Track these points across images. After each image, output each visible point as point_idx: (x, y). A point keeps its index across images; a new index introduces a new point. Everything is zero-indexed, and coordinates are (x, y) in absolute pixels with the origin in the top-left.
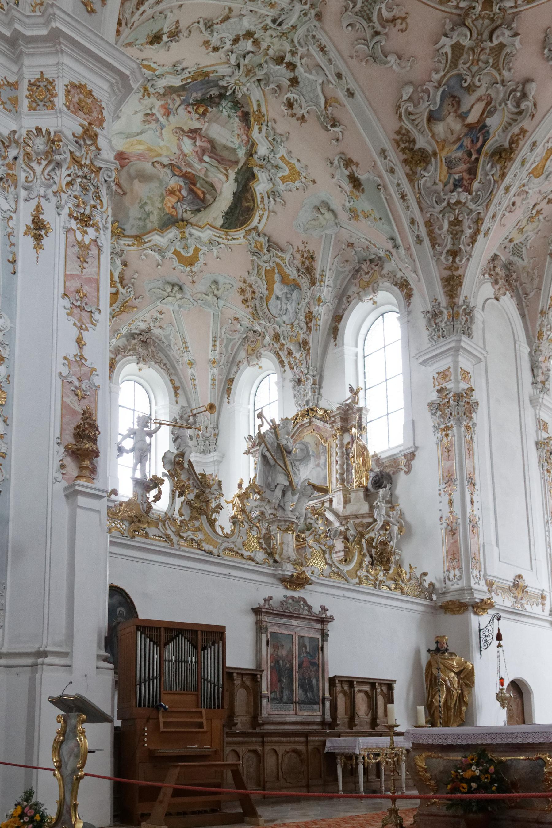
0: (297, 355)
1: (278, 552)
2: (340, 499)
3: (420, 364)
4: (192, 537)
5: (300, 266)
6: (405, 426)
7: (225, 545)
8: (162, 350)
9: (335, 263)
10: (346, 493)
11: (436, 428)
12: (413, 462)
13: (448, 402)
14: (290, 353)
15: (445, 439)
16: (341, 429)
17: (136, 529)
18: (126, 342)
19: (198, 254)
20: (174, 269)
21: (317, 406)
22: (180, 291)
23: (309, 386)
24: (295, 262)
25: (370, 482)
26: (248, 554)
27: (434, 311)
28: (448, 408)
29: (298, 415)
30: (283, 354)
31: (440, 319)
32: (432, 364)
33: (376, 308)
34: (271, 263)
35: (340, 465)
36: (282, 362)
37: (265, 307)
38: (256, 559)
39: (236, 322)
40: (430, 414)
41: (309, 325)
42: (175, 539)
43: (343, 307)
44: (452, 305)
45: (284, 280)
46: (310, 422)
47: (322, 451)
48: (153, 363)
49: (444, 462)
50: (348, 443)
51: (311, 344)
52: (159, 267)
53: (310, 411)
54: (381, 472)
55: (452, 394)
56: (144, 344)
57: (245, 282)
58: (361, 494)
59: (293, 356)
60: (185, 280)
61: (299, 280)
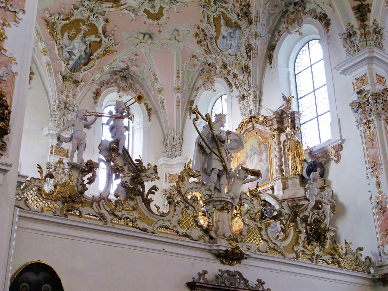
0: (241, 77)
1: (214, 229)
2: (279, 186)
3: (341, 73)
4: (127, 215)
5: (239, 12)
6: (331, 124)
7: (160, 223)
8: (138, 82)
9: (267, 7)
10: (285, 180)
11: (359, 123)
12: (341, 153)
13: (368, 101)
14: (235, 76)
15: (367, 131)
16: (278, 129)
17: (70, 209)
18: (110, 78)
19: (162, 11)
20: (145, 23)
21: (258, 114)
22: (150, 39)
23: (251, 100)
24: (235, 9)
25: (305, 171)
26: (184, 231)
27: (349, 32)
28: (368, 105)
29: (243, 122)
30: (230, 78)
31: (355, 38)
32: (351, 73)
33: (301, 38)
34: (217, 12)
35: (279, 158)
36: (230, 85)
37: (215, 44)
38: (192, 235)
39: (194, 58)
40: (352, 112)
41: (249, 54)
42: (109, 217)
43: (276, 39)
44: (363, 26)
45: (228, 23)
46: (253, 127)
47: (263, 149)
48: (130, 92)
49: (369, 150)
50: (285, 141)
51: (251, 68)
52: (133, 22)
53: (252, 119)
54: (314, 162)
55: (370, 94)
56: (124, 79)
57: (199, 28)
58: (297, 180)
59: (238, 78)
60: (154, 30)
61: (239, 22)
